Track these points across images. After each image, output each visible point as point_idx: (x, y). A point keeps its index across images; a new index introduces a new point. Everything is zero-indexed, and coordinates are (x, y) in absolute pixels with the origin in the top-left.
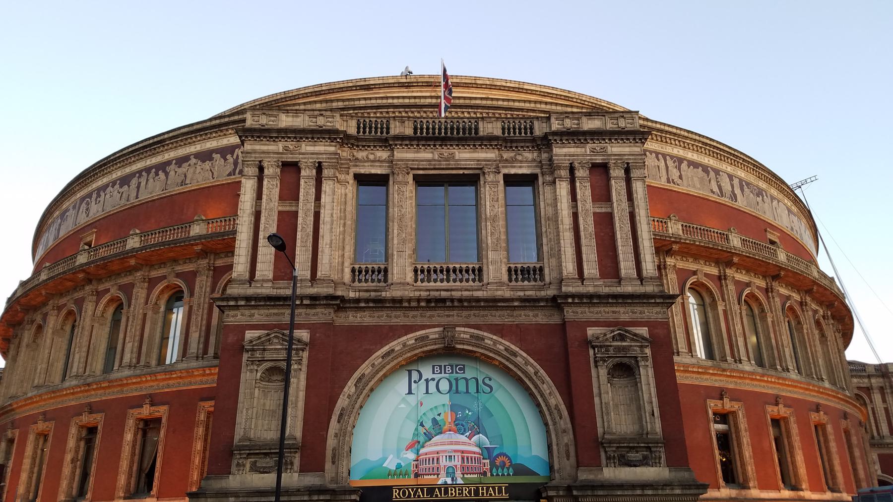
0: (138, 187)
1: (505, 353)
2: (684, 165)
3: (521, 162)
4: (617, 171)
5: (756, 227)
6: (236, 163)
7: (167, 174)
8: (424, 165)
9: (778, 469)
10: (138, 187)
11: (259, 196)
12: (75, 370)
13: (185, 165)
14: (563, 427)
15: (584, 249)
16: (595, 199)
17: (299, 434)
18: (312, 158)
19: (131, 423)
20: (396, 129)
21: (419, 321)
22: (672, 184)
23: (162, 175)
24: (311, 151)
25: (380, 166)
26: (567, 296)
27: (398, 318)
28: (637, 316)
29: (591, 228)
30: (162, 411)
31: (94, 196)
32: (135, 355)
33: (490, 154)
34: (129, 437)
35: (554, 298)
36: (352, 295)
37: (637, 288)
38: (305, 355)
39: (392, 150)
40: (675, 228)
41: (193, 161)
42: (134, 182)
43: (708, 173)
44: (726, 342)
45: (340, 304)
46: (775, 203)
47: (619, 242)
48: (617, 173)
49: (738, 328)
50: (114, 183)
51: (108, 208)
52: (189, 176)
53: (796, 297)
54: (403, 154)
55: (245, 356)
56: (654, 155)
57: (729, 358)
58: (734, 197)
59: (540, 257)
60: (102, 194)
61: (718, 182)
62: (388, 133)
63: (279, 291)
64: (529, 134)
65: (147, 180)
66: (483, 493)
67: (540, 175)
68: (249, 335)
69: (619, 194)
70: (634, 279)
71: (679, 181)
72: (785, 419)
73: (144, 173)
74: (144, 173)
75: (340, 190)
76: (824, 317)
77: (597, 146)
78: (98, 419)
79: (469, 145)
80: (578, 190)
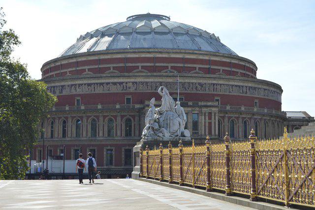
6: (123, 87)
19: (105, 150)
23: (102, 86)
30: (113, 148)
34: (105, 153)
40: (228, 108)
41: (111, 84)
42: (93, 86)
48: (213, 114)
60: (81, 87)
78: (95, 148)
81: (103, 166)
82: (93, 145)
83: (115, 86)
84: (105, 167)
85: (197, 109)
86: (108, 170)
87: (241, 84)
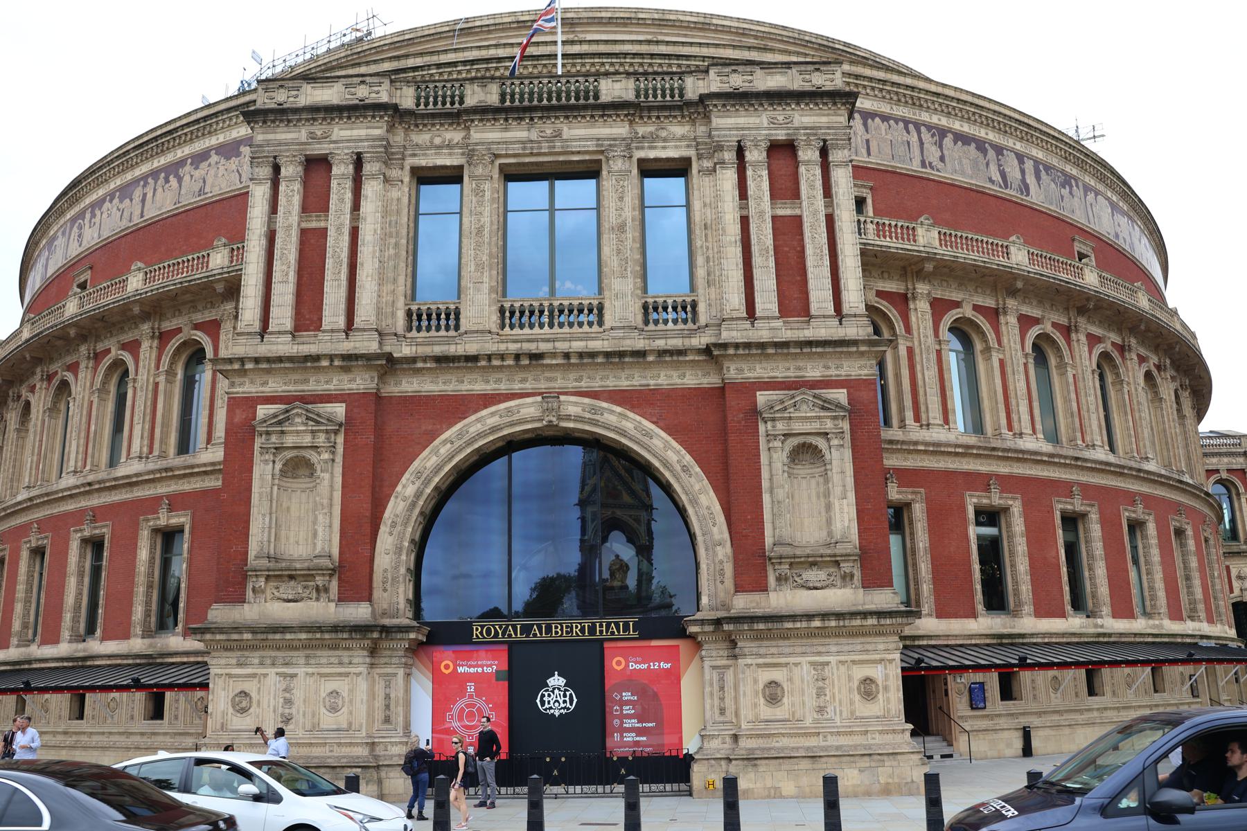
0: (143, 201)
1: (633, 432)
2: (948, 141)
3: (665, 140)
4: (809, 152)
5: (1056, 233)
7: (180, 180)
8: (517, 149)
9: (1067, 588)
10: (143, 201)
11: (274, 209)
12: (72, 463)
13: (204, 165)
14: (717, 537)
15: (757, 273)
16: (776, 194)
17: (336, 552)
18: (348, 148)
20: (474, 96)
21: (503, 387)
22: (929, 170)
23: (173, 181)
24: (347, 137)
25: (450, 154)
26: (725, 346)
27: (473, 384)
28: (833, 372)
29: (769, 241)
31: (88, 216)
32: (146, 442)
33: (617, 129)
34: (143, 554)
35: (707, 350)
36: (406, 351)
37: (833, 331)
38: (340, 439)
39: (468, 128)
40: (927, 238)
41: (214, 158)
42: (138, 193)
43: (985, 152)
44: (1002, 407)
45: (389, 365)
46: (1091, 196)
47: (810, 262)
48: (808, 155)
49: (1022, 385)
50: (111, 196)
51: (106, 234)
52: (209, 181)
53: (1114, 337)
54: (487, 134)
55: (258, 442)
56: (901, 125)
57: (1005, 431)
58: (1025, 188)
59: (693, 288)
61: (1000, 166)
62: (461, 102)
63: (301, 347)
64: (677, 98)
65: (155, 190)
66: (601, 632)
67: (694, 159)
68: (262, 411)
69: (812, 187)
70: (829, 317)
71: (940, 165)
72: (1084, 516)
73: (150, 180)
74: (150, 180)
75: (394, 193)
76: (1158, 367)
77: (780, 114)
78: (104, 530)
79: (584, 117)
80: (750, 182)
81: (126, 636)
82: (96, 514)
83: (233, 163)
84: (137, 644)
85: (678, 129)
86: (151, 661)
87: (992, 136)
